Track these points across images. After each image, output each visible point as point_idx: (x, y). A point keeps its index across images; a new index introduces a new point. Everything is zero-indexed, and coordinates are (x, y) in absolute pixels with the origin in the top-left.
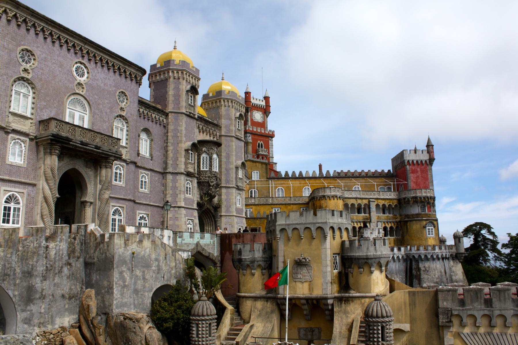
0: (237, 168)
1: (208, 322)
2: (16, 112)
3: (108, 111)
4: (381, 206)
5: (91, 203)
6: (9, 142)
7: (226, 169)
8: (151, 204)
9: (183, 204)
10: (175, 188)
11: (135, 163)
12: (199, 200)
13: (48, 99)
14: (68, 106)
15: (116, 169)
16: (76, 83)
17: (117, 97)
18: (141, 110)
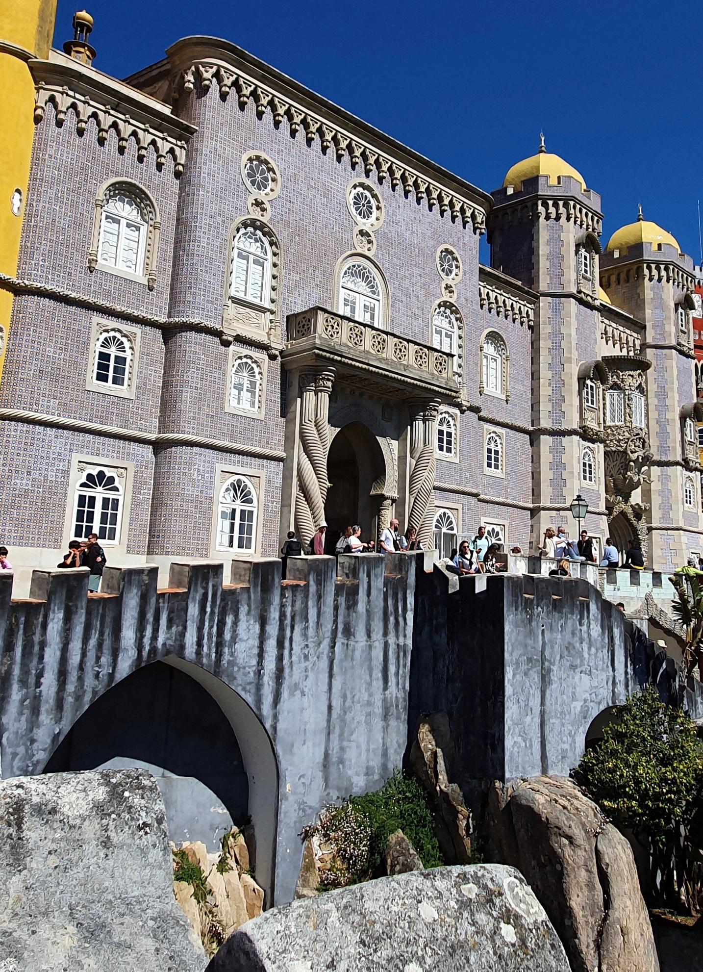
0: (683, 418)
2: (241, 295)
3: (423, 292)
5: (394, 501)
6: (230, 365)
7: (658, 422)
8: (509, 501)
10: (559, 465)
13: (303, 266)
14: (341, 284)
16: (356, 231)
18: (484, 291)
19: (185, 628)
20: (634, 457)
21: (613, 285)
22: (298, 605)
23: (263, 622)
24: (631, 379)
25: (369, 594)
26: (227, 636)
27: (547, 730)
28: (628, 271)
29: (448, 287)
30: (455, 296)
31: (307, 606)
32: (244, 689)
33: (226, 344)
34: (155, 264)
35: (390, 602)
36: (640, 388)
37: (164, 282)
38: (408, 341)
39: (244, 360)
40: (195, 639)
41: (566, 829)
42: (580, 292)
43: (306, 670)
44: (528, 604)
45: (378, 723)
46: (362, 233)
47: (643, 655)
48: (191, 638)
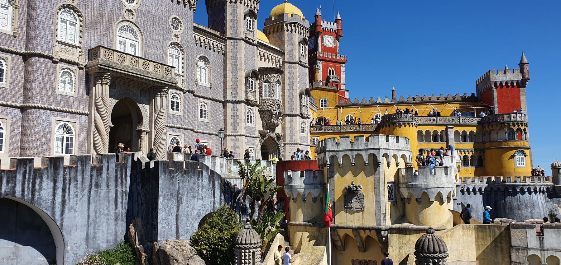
0: (301, 95)
1: (251, 250)
2: (63, 40)
4: (461, 133)
5: (147, 132)
6: (58, 72)
7: (289, 97)
8: (212, 132)
9: (244, 133)
10: (235, 117)
11: (192, 92)
12: (261, 129)
14: (117, 34)
15: (173, 97)
16: (125, 9)
17: (170, 23)
18: (197, 37)
19: (15, 185)
20: (275, 112)
21: (272, 33)
22: (72, 175)
23: (55, 182)
24: (274, 78)
25: (108, 170)
26: (37, 187)
27: (179, 221)
28: (278, 27)
29: (175, 35)
30: (180, 39)
31: (77, 176)
32: (46, 209)
33: (56, 63)
34: (16, 25)
35: (119, 173)
36: (278, 82)
37: (22, 34)
38: (150, 61)
39: (66, 70)
40: (21, 189)
41: (175, 257)
42: (246, 37)
43: (77, 201)
44: (171, 172)
45: (112, 223)
46: (128, 10)
47: (228, 190)
48: (18, 189)
